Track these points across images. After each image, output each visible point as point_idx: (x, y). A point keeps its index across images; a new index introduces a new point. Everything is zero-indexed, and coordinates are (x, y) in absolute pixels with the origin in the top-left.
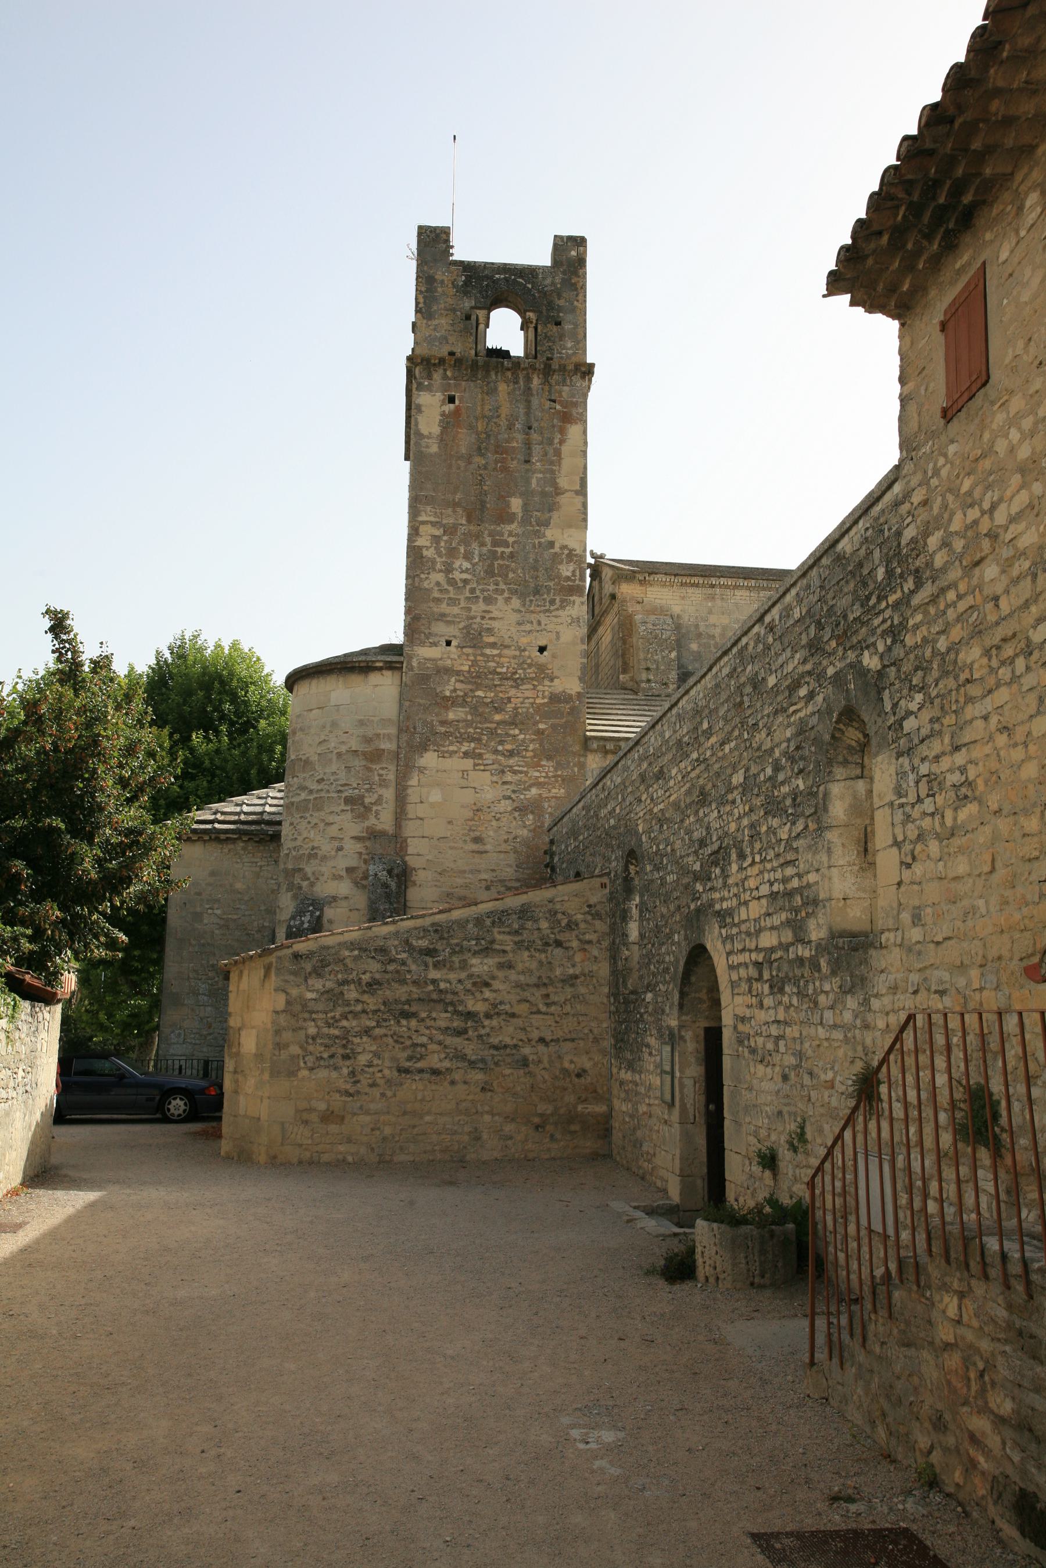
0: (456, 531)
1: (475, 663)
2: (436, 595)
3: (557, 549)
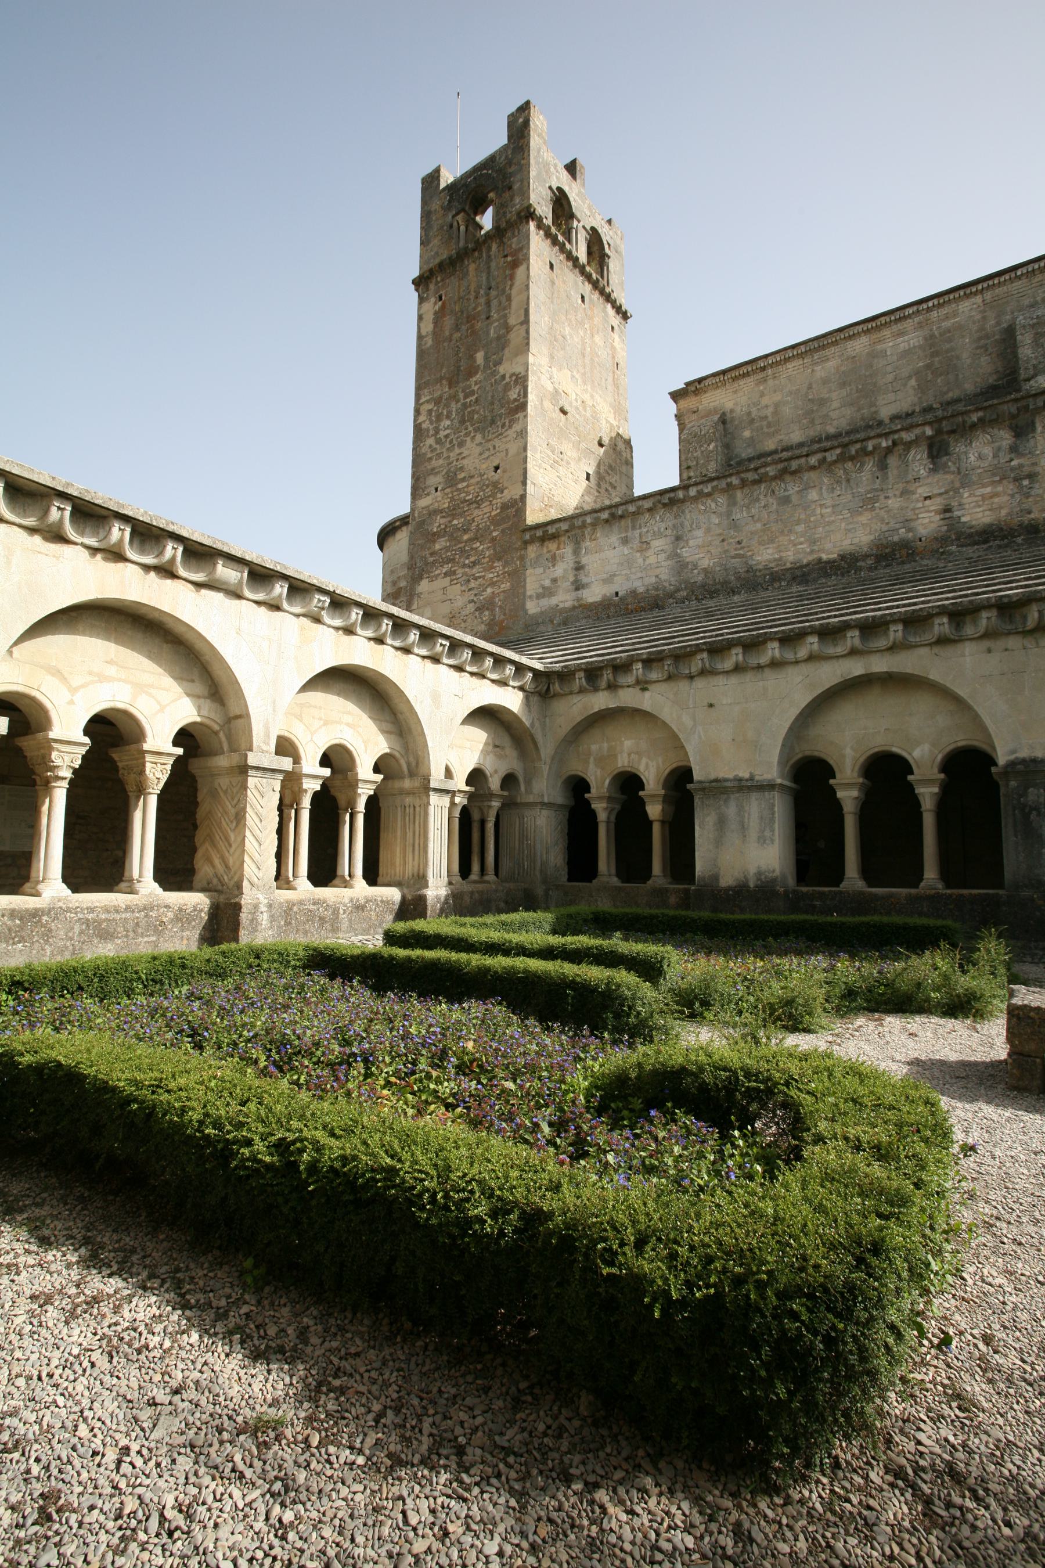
1: (452, 499)
2: (429, 455)
3: (507, 379)
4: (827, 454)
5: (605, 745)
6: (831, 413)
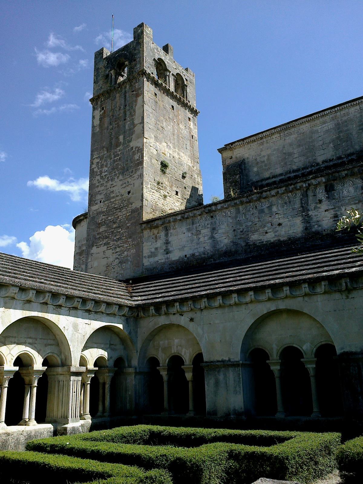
0: (103, 157)
2: (97, 185)
3: (134, 149)
4: (279, 190)
5: (166, 341)
6: (294, 160)
